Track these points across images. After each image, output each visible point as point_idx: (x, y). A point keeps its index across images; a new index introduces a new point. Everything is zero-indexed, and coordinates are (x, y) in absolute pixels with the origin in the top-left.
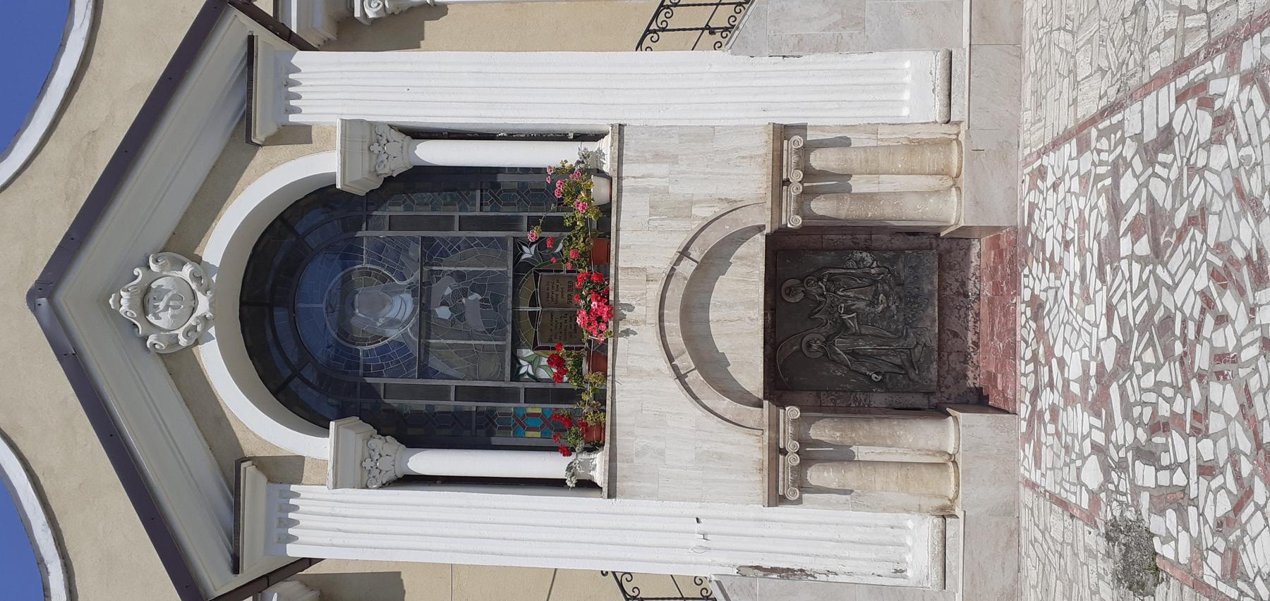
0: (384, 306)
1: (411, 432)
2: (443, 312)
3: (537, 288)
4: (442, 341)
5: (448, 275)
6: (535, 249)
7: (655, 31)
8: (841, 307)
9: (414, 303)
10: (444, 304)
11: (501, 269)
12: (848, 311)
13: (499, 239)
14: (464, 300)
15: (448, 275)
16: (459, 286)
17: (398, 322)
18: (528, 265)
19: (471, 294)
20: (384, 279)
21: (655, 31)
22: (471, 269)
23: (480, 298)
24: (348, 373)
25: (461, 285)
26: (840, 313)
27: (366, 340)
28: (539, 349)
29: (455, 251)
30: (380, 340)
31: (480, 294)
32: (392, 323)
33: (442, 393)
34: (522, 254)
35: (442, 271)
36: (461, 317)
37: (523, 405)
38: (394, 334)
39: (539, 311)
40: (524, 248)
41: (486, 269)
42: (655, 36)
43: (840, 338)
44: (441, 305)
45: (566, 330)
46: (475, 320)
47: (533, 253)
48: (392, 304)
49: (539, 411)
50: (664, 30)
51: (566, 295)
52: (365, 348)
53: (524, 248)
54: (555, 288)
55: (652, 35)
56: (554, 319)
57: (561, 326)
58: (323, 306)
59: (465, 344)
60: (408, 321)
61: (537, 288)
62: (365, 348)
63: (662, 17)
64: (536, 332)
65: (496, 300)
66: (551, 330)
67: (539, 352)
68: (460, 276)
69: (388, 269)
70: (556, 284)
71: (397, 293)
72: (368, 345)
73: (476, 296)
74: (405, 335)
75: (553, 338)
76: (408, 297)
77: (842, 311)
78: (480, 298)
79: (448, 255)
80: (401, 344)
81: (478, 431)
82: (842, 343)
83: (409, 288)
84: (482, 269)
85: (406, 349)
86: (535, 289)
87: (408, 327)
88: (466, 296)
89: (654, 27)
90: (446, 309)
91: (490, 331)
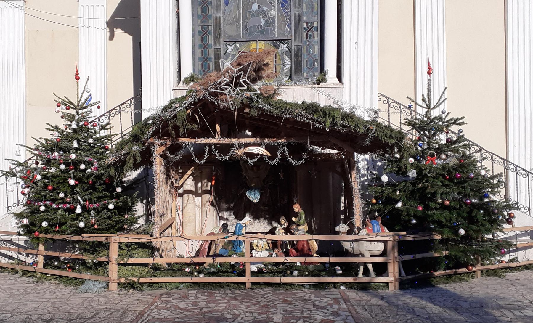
4: (242, 7)
7: (388, 102)
8: (262, 191)
10: (259, 7)
19: (264, 20)
21: (388, 102)
22: (276, 19)
31: (264, 24)
33: (218, 7)
34: (283, 44)
36: (253, 16)
40: (286, 45)
42: (387, 102)
44: (259, 6)
46: (252, 22)
49: (210, 56)
50: (389, 106)
53: (286, 45)
55: (387, 100)
59: (241, 18)
63: (395, 105)
65: (262, 32)
73: (263, 22)
81: (201, 27)
89: (390, 101)
90: (257, 7)
91: (247, 30)
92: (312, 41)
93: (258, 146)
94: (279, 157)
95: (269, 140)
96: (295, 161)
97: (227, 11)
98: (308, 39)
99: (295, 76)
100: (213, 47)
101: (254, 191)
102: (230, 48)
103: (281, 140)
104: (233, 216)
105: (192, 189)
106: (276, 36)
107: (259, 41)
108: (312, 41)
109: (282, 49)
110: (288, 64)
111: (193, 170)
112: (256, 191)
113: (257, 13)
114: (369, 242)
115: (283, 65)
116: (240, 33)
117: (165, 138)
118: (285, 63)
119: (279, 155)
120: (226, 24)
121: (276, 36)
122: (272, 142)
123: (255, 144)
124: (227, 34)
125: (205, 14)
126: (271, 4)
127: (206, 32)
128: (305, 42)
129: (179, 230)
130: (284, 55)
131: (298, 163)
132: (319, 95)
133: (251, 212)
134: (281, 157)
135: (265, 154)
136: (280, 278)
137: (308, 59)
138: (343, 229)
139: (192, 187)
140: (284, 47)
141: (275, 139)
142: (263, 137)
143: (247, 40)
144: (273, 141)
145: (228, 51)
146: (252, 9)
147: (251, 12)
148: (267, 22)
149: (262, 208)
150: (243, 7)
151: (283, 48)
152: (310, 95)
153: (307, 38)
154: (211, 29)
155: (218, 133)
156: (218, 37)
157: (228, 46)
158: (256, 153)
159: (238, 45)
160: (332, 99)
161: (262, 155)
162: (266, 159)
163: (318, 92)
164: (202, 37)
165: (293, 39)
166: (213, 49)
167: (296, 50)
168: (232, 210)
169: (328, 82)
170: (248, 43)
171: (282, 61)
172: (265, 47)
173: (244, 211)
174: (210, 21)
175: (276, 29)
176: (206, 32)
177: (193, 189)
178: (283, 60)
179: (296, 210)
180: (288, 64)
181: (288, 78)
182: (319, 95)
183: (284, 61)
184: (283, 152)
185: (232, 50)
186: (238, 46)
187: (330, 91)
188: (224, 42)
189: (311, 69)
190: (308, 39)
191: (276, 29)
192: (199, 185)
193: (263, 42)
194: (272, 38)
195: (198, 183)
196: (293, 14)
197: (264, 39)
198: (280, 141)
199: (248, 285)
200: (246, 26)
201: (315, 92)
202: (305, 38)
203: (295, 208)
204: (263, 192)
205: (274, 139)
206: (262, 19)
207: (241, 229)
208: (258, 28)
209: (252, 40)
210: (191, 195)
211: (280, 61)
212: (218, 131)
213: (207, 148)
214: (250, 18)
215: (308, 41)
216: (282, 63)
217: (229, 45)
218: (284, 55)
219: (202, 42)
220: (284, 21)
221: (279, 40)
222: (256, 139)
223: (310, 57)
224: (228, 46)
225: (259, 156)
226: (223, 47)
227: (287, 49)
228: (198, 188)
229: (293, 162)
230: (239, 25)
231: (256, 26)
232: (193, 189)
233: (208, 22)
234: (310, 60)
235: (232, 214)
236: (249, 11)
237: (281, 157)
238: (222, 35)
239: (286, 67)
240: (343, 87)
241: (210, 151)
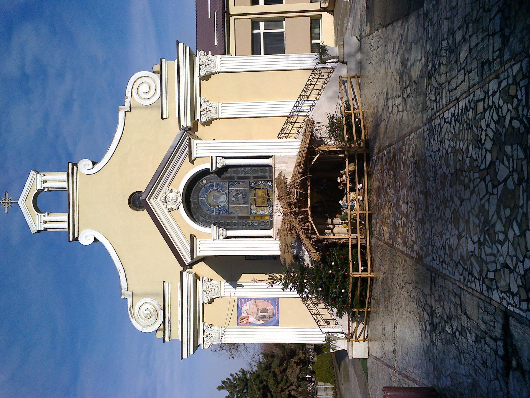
1: (227, 227)
2: (234, 199)
10: (234, 197)
17: (223, 202)
25: (237, 193)
29: (236, 185)
32: (222, 202)
33: (234, 218)
36: (238, 200)
38: (222, 204)
41: (243, 188)
46: (241, 201)
48: (221, 197)
52: (216, 208)
58: (205, 198)
62: (216, 208)
65: (246, 195)
67: (257, 208)
68: (237, 190)
73: (241, 195)
74: (225, 204)
91: (245, 203)
130: (257, 184)
140: (253, 184)
154: (244, 221)
156: (248, 217)
165: (249, 180)
196: (238, 180)
218: (257, 184)
233: (241, 222)
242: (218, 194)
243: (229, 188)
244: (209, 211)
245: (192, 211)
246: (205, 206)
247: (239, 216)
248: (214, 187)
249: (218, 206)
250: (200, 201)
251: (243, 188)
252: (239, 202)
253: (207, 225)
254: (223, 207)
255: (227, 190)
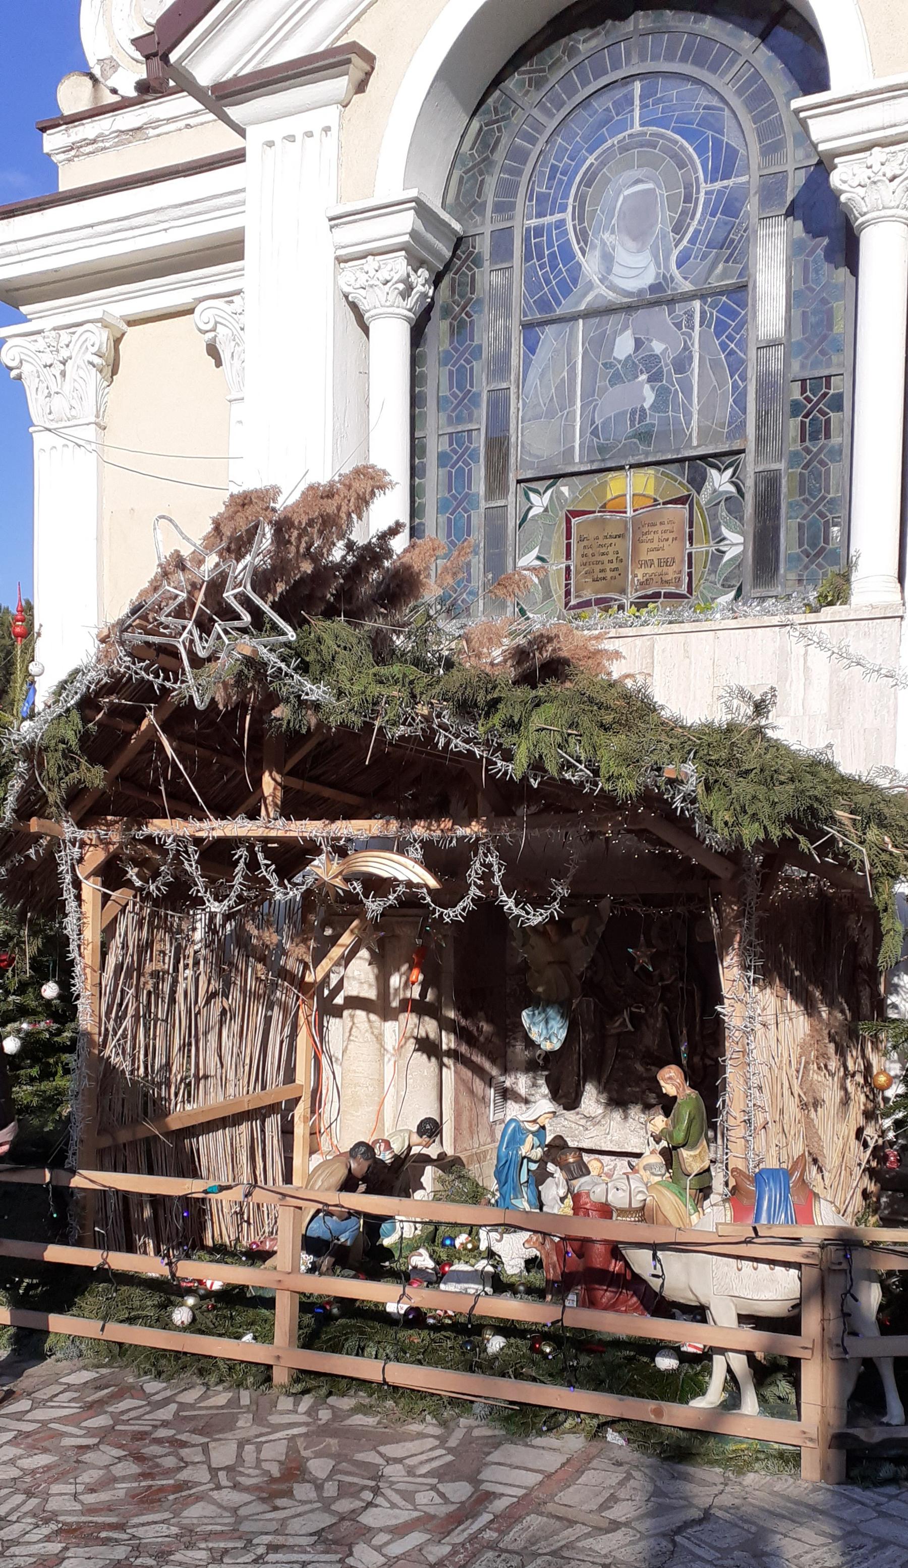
0: (635, 239)
2: (624, 346)
3: (664, 503)
5: (685, 342)
6: (727, 492)
8: (639, 1008)
9: (641, 292)
10: (638, 343)
11: (695, 434)
12: (633, 1017)
13: (743, 424)
14: (644, 377)
15: (685, 342)
16: (667, 365)
17: (609, 270)
18: (698, 481)
19: (653, 388)
20: (679, 228)
23: (647, 406)
24: (531, 200)
25: (667, 367)
26: (631, 1006)
27: (581, 221)
28: (568, 522)
30: (582, 244)
31: (652, 405)
32: (608, 259)
34: (719, 469)
35: (692, 329)
36: (616, 379)
37: (483, 505)
38: (590, 266)
39: (625, 512)
40: (730, 472)
41: (695, 408)
43: (595, 1003)
45: (598, 563)
47: (721, 489)
51: (653, 556)
53: (730, 472)
54: (665, 536)
56: (613, 541)
57: (603, 554)
59: (575, 392)
60: (612, 287)
61: (664, 503)
64: (594, 512)
66: (597, 538)
68: (682, 364)
69: (697, 232)
70: (671, 536)
71: (656, 257)
72: (574, 226)
73: (649, 396)
74: (590, 286)
75: (585, 543)
76: (649, 278)
77: (634, 1010)
78: (647, 406)
79: (718, 335)
80: (575, 281)
82: (588, 1006)
83: (664, 275)
84: (695, 400)
85: (567, 292)
86: (661, 501)
87: (603, 290)
88: (649, 380)
91: (595, 433)
92: (821, 450)
93: (390, 850)
94: (474, 891)
95: (429, 828)
96: (529, 908)
97: (533, 373)
98: (807, 443)
99: (755, 586)
100: (483, 505)
101: (544, 1011)
102: (539, 503)
103: (468, 825)
104: (545, 1090)
105: (364, 994)
106: (695, 443)
107: (632, 466)
108: (821, 450)
109: (715, 491)
110: (733, 545)
111: (356, 931)
112: (551, 1012)
113: (631, 367)
114: (732, 1261)
115: (718, 550)
116: (573, 447)
117: (109, 818)
118: (724, 539)
119: (475, 883)
120: (527, 418)
121: (695, 443)
122: (439, 833)
123: (382, 844)
124: (530, 454)
125: (461, 391)
126: (680, 329)
127: (463, 454)
128: (796, 454)
129: (333, 1126)
131: (536, 919)
132: (806, 652)
133: (604, 1080)
134: (480, 894)
135: (416, 880)
136: (380, 1364)
137: (804, 518)
138: (620, 1194)
139: (366, 986)
141: (450, 825)
142: (409, 816)
143: (594, 468)
144: (442, 831)
145: (531, 514)
146: (615, 354)
147: (611, 365)
148: (663, 396)
149: (639, 1067)
150: (585, 353)
151: (717, 486)
152: (774, 653)
153: (803, 440)
154: (480, 442)
155: (265, 799)
157: (532, 496)
158: (385, 875)
159: (565, 490)
160: (858, 664)
161: (409, 884)
162: (424, 899)
163: (804, 642)
164: (450, 473)
165: (751, 446)
166: (482, 510)
167: (762, 486)
168: (544, 1068)
169: (854, 599)
170: (596, 478)
171: (713, 532)
172: (656, 491)
173: (579, 1075)
174: (475, 416)
175: (695, 417)
176: (463, 454)
177: (371, 993)
178: (716, 530)
179: (669, 1089)
180: (733, 545)
181: (732, 594)
182: (806, 652)
183: (721, 534)
184: (487, 876)
185: (546, 510)
186: (567, 494)
187: (852, 633)
188: (519, 482)
189: (818, 555)
190: (807, 443)
191: (695, 417)
192: (395, 981)
193: (651, 471)
194: (678, 451)
195: (390, 975)
197: (650, 459)
198: (467, 831)
199: (280, 1376)
200: (593, 418)
201: (794, 640)
202: (795, 441)
203: (662, 1083)
204: (643, 1011)
205: (447, 824)
206: (647, 387)
207: (523, 1142)
208: (632, 421)
209: (609, 464)
210: (360, 1014)
211: (706, 533)
212: (266, 794)
213: (242, 852)
214: (607, 389)
215: (808, 451)
216: (712, 543)
217: (536, 491)
219: (450, 490)
220: (722, 384)
221: (703, 458)
222: (388, 822)
223: (812, 510)
224: (532, 496)
225: (401, 889)
226: (511, 501)
227: (732, 489)
228: (392, 991)
229: (516, 911)
230: (570, 417)
231: (625, 413)
232: (371, 993)
233: (471, 415)
234: (812, 524)
235: (541, 1082)
236: (604, 365)
237: (480, 894)
238: (512, 460)
239: (727, 557)
240: (902, 617)
241: (253, 865)
242: (663, 220)
243: (702, 297)
244: (552, 177)
245: (557, 49)
246: (585, 139)
247: (507, 399)
248: (718, 185)
249: (582, 236)
250: (618, 93)
251: (695, 408)
252: (604, 390)
253: (461, 178)
254: (576, 272)
255: (687, 286)
